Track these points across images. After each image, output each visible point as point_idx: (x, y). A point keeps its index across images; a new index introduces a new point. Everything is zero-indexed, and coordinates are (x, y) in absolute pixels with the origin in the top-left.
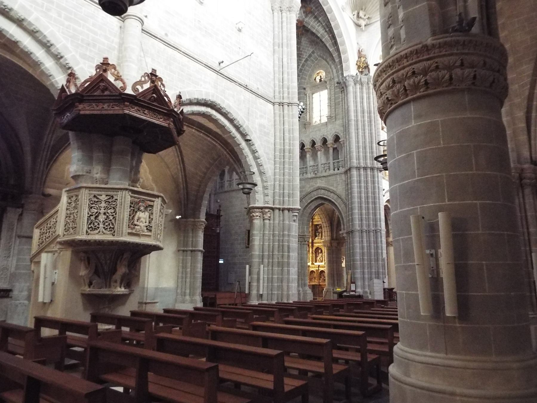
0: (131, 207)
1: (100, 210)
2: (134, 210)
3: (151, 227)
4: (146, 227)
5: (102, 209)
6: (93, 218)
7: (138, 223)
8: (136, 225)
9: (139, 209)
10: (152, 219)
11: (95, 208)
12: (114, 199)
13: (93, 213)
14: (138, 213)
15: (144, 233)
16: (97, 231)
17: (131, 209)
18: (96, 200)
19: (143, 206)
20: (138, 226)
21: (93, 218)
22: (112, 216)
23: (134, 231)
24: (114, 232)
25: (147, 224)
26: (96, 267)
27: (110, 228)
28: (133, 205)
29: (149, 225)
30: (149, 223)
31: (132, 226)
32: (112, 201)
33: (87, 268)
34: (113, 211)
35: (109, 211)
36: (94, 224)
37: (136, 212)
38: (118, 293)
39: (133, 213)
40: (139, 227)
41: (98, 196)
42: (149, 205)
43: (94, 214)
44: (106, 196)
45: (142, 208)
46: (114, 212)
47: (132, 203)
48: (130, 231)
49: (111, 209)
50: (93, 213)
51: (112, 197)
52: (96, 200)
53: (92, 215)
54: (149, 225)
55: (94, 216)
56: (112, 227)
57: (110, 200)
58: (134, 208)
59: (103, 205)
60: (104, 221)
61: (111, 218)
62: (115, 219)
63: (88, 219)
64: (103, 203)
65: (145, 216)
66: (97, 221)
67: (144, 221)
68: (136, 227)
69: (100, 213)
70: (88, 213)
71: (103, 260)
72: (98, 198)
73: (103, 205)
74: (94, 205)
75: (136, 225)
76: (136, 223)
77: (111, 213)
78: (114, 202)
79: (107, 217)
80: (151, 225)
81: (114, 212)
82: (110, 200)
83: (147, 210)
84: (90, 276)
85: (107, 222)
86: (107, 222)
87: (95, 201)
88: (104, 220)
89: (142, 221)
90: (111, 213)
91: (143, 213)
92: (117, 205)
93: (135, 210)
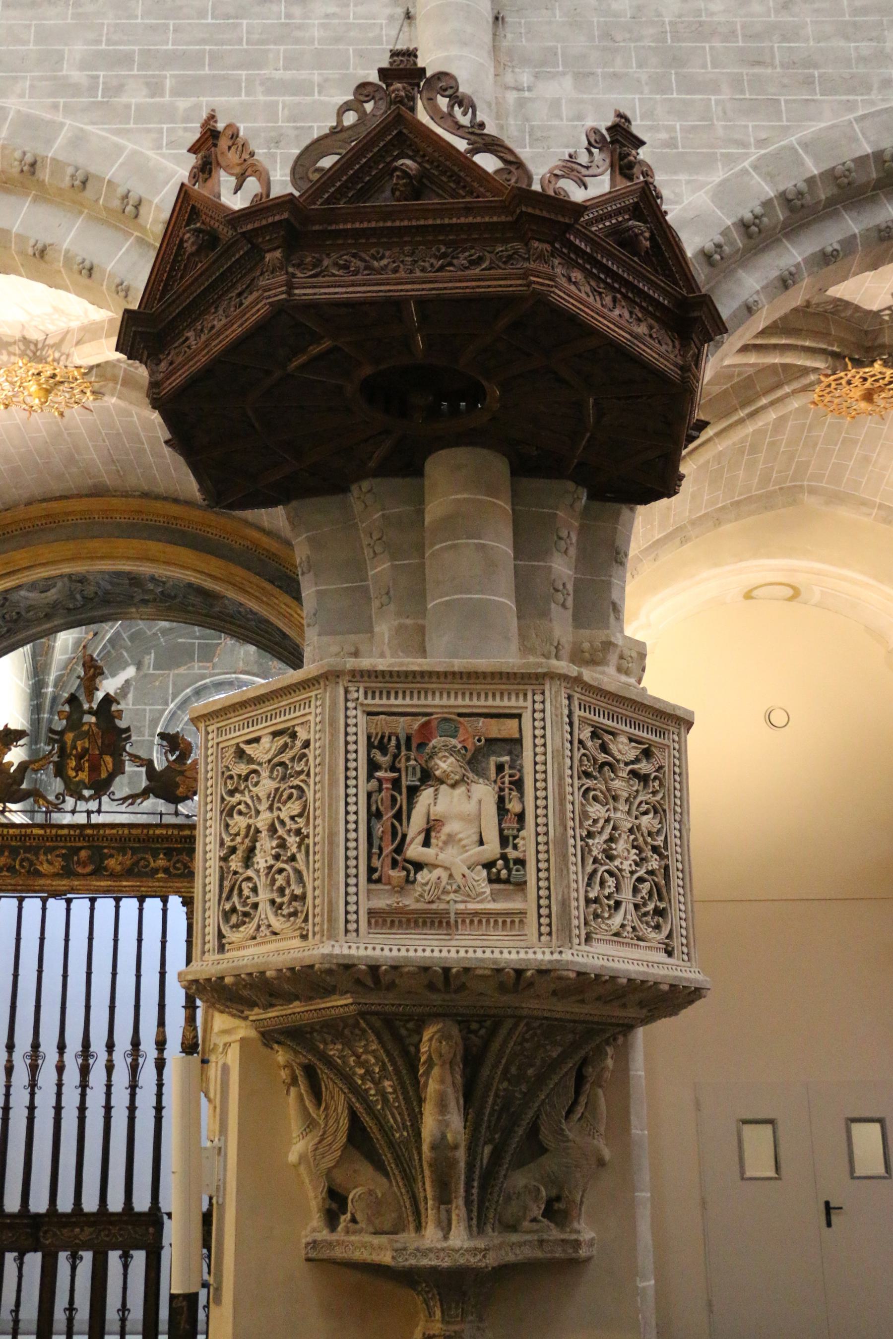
0: (373, 766)
1: (258, 812)
2: (396, 784)
3: (521, 862)
4: (489, 866)
5: (263, 807)
6: (235, 863)
7: (427, 853)
8: (419, 866)
9: (427, 777)
10: (521, 817)
11: (242, 807)
12: (298, 744)
13: (238, 834)
14: (426, 796)
15: (472, 906)
16: (249, 929)
17: (380, 780)
18: (242, 768)
19: (452, 751)
20: (435, 866)
21: (235, 863)
22: (298, 832)
23: (409, 902)
24: (306, 920)
25: (492, 848)
26: (354, 1117)
27: (294, 898)
28: (383, 760)
29: (504, 857)
30: (504, 841)
31: (397, 875)
32: (292, 759)
33: (310, 1124)
34: (294, 807)
35: (284, 815)
36: (241, 890)
37: (413, 792)
38: (425, 1262)
39: (394, 800)
40: (437, 872)
41: (249, 750)
42: (490, 741)
43: (239, 839)
44: (276, 734)
45: (444, 765)
46: (300, 815)
47: (383, 749)
48: (382, 902)
49: (290, 797)
50: (238, 834)
51: (294, 736)
52: (242, 768)
53: (233, 850)
54: (504, 857)
55: (240, 853)
56: (298, 891)
57: (285, 757)
58: (393, 768)
59: (266, 785)
60: (271, 867)
61: (292, 841)
62: (308, 846)
63: (221, 868)
64: (265, 774)
65: (470, 807)
66: (250, 873)
67: (468, 834)
68: (423, 876)
69: (258, 831)
70: (222, 844)
71: (362, 1077)
72: (250, 760)
73: (266, 785)
74: (238, 797)
75: (419, 866)
76: (414, 850)
77: (292, 818)
78: (300, 759)
79: (283, 845)
80: (512, 854)
81: (300, 815)
82: (285, 757)
83: (481, 773)
84: (328, 1162)
85: (281, 871)
86: (281, 871)
87: (239, 776)
88: (273, 862)
89: (451, 839)
90: (292, 818)
91: (462, 789)
92: (308, 775)
93: (404, 783)
